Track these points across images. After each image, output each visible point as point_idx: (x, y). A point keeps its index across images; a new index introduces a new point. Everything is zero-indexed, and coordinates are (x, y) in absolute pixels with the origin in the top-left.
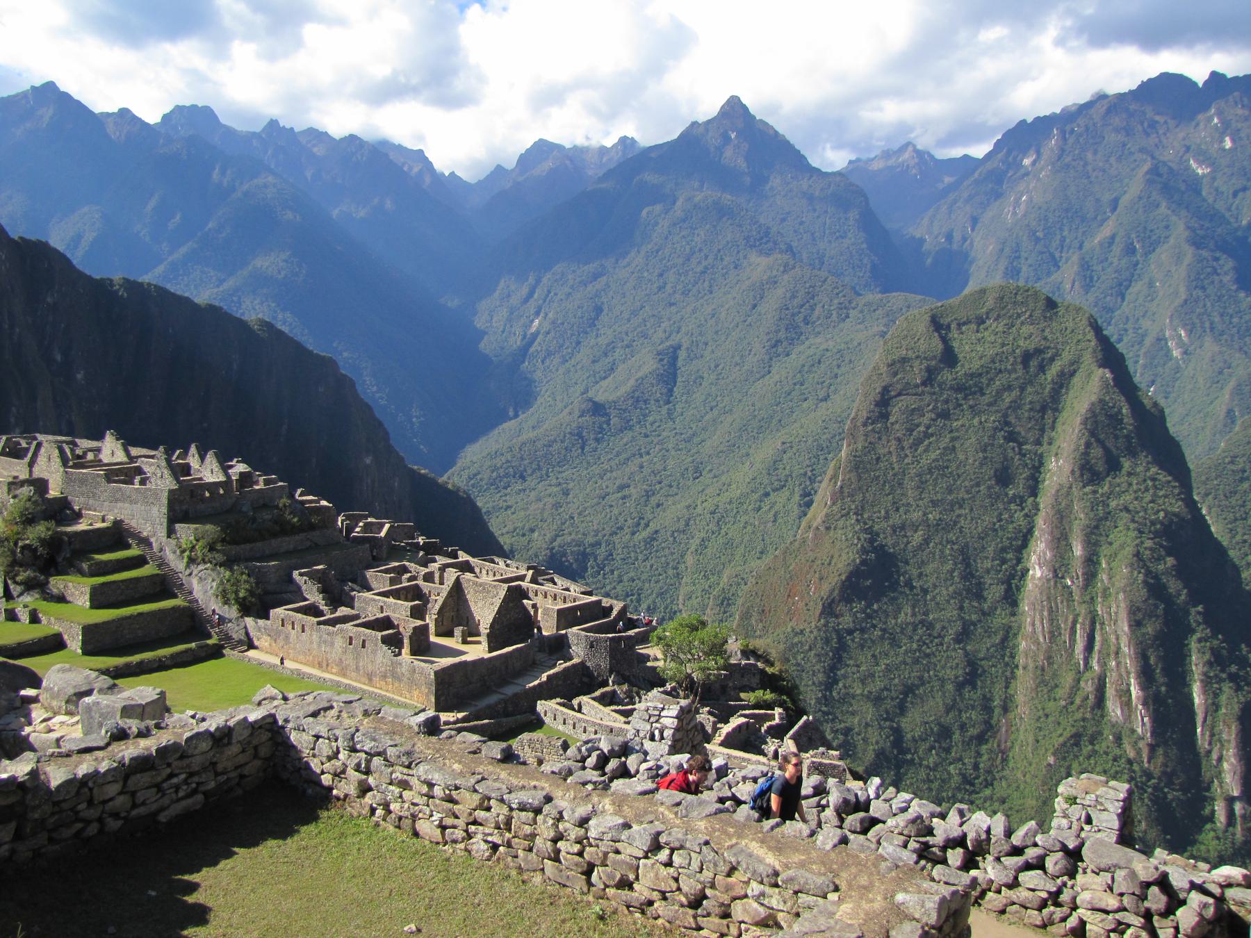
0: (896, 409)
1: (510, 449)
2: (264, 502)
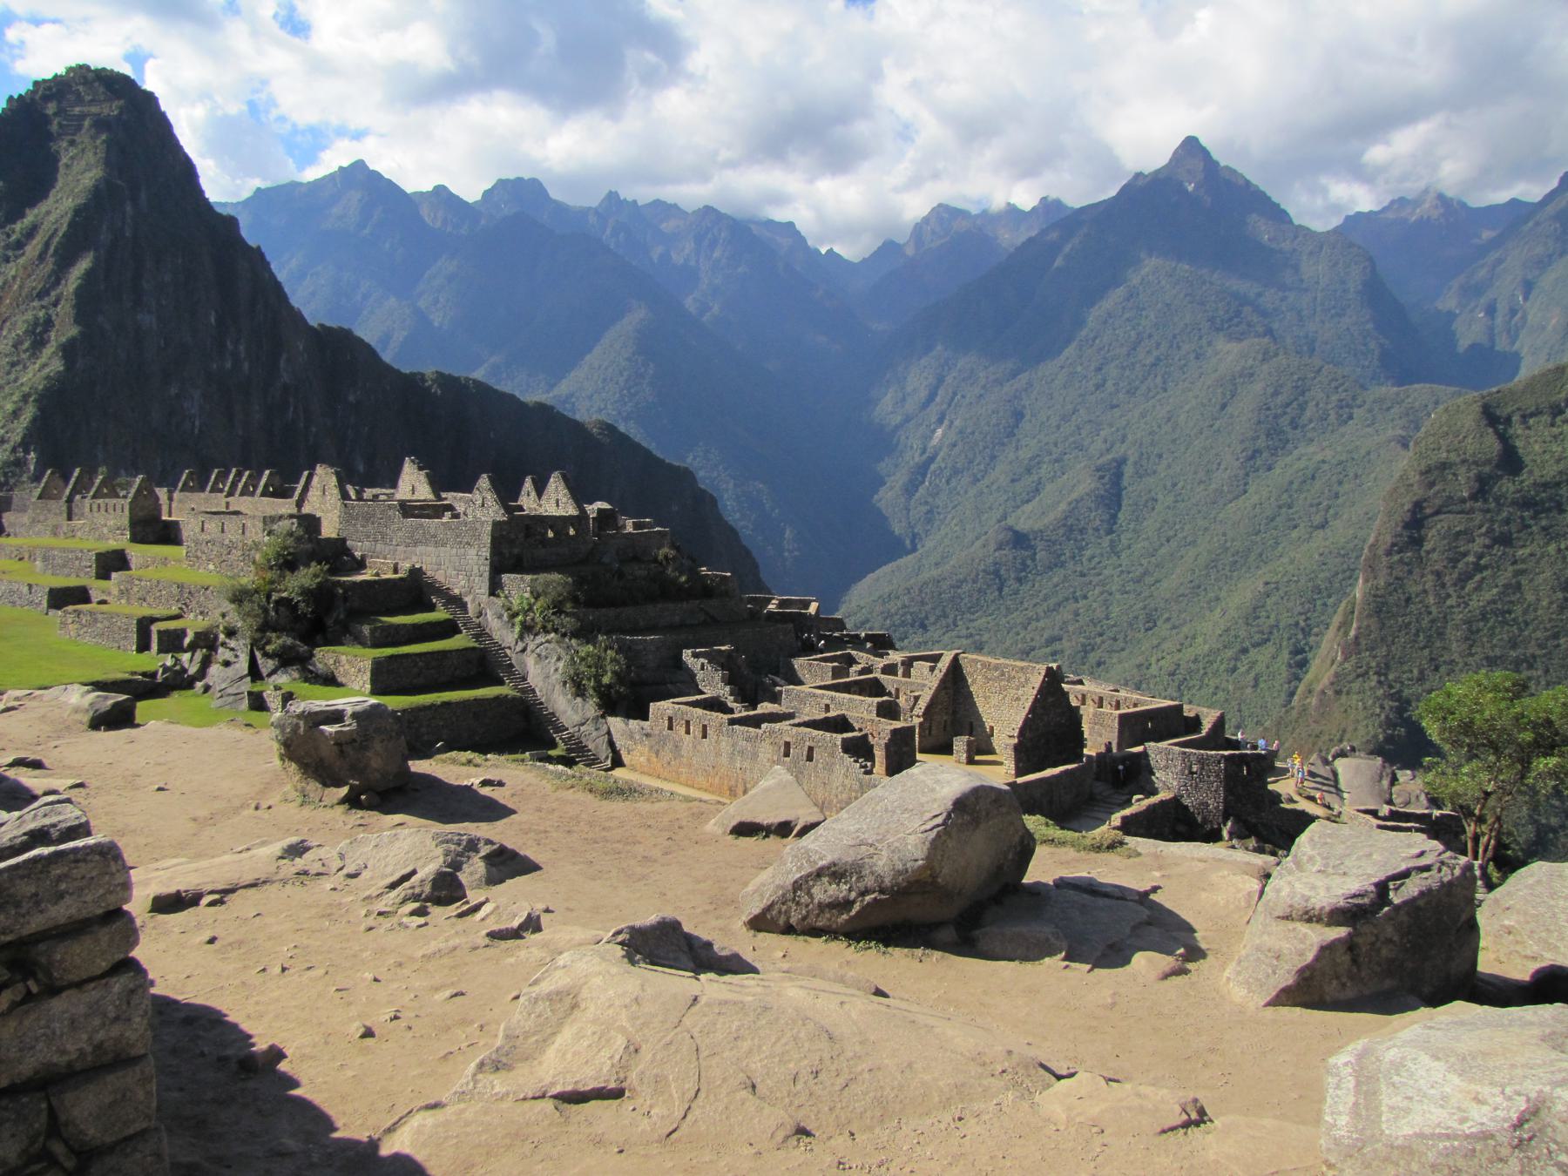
0: (1434, 532)
1: (908, 590)
2: (635, 551)
